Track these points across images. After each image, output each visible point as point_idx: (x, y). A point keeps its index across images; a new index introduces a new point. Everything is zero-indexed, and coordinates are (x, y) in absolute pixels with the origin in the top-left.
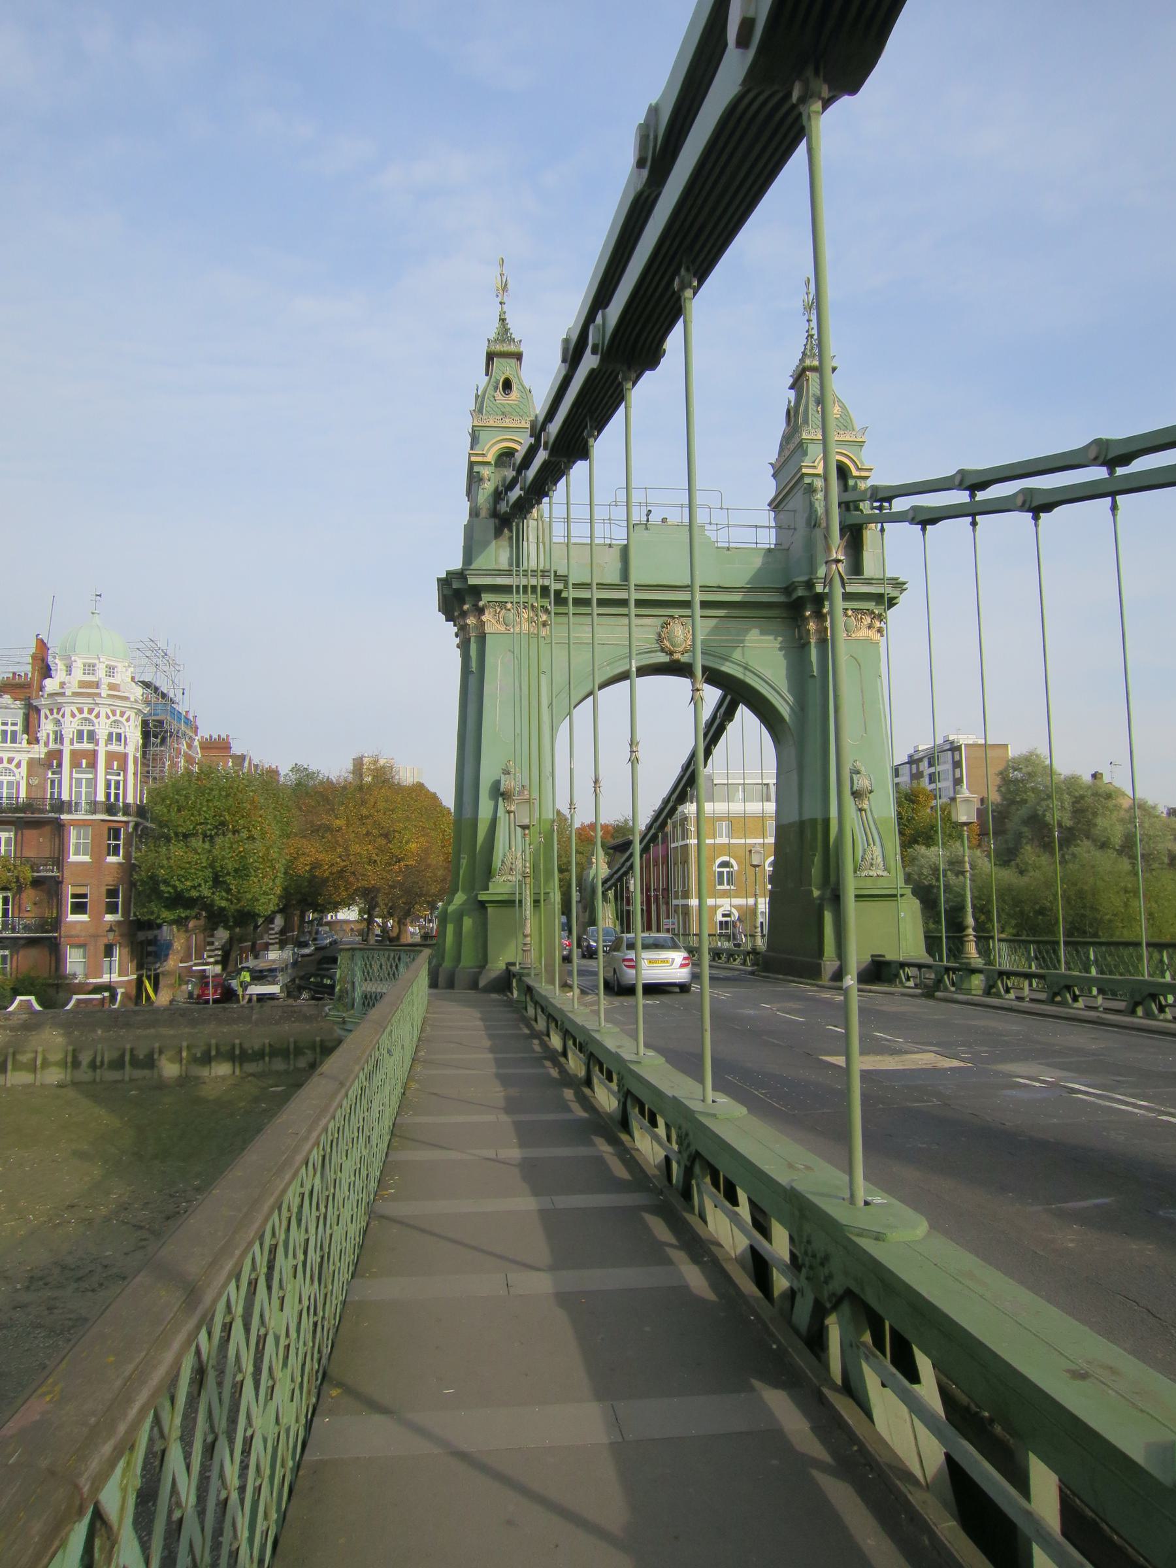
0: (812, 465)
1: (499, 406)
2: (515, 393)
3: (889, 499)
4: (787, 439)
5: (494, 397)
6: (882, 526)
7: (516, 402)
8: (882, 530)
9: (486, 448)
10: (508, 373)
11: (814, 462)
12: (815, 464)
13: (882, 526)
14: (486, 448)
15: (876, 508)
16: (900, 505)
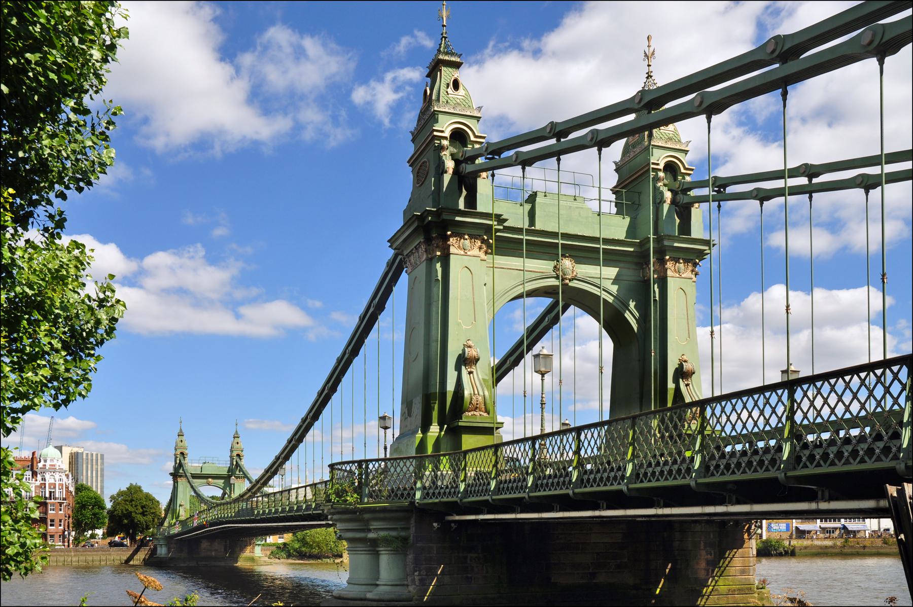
0: (657, 162)
1: (452, 99)
2: (461, 91)
3: (725, 186)
4: (423, 112)
5: (447, 92)
6: (719, 204)
7: (463, 97)
8: (719, 206)
9: (445, 127)
10: (456, 76)
11: (658, 161)
12: (659, 162)
13: (719, 204)
14: (445, 127)
15: (715, 191)
16: (731, 189)
